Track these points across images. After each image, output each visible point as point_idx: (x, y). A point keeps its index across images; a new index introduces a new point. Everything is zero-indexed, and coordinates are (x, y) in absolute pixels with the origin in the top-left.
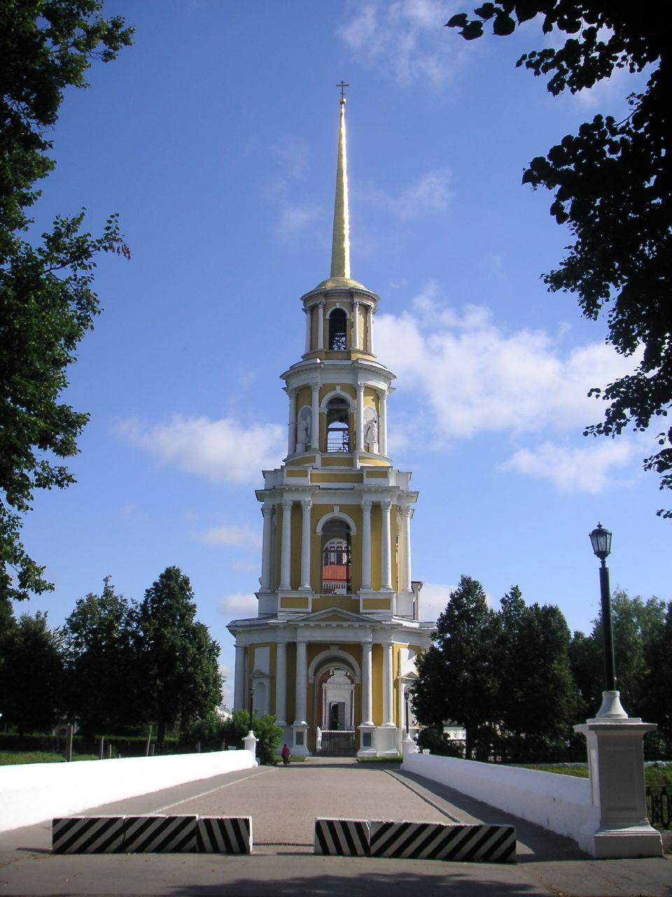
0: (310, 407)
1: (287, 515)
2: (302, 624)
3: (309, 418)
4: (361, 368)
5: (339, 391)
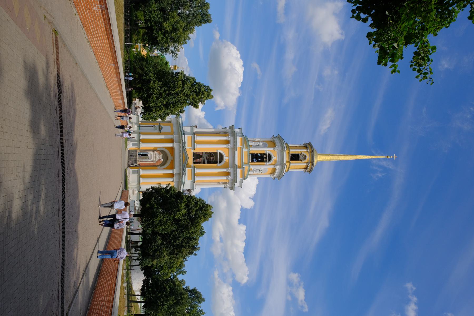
0: (267, 147)
1: (224, 138)
2: (181, 145)
4: (283, 167)
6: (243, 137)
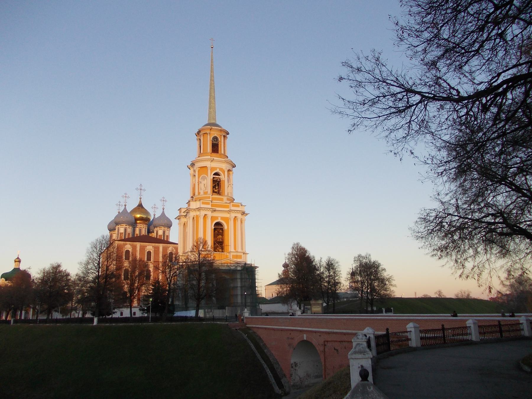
3: (206, 180)
5: (218, 171)
6: (201, 201)
